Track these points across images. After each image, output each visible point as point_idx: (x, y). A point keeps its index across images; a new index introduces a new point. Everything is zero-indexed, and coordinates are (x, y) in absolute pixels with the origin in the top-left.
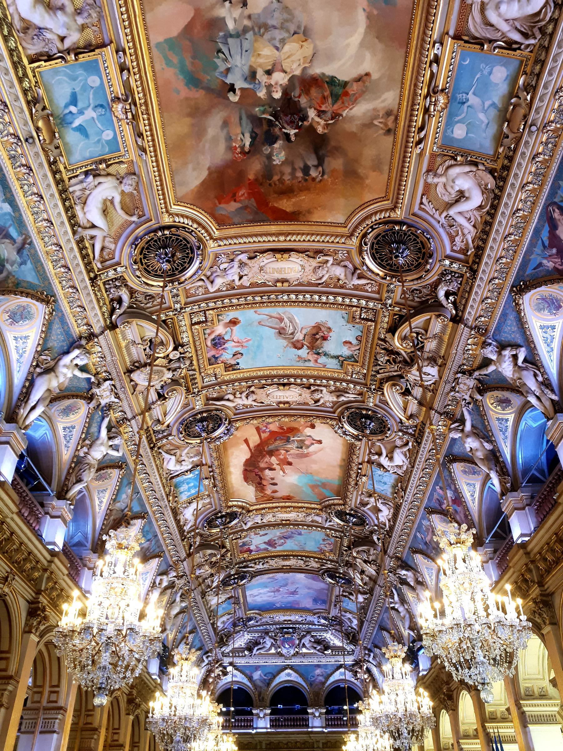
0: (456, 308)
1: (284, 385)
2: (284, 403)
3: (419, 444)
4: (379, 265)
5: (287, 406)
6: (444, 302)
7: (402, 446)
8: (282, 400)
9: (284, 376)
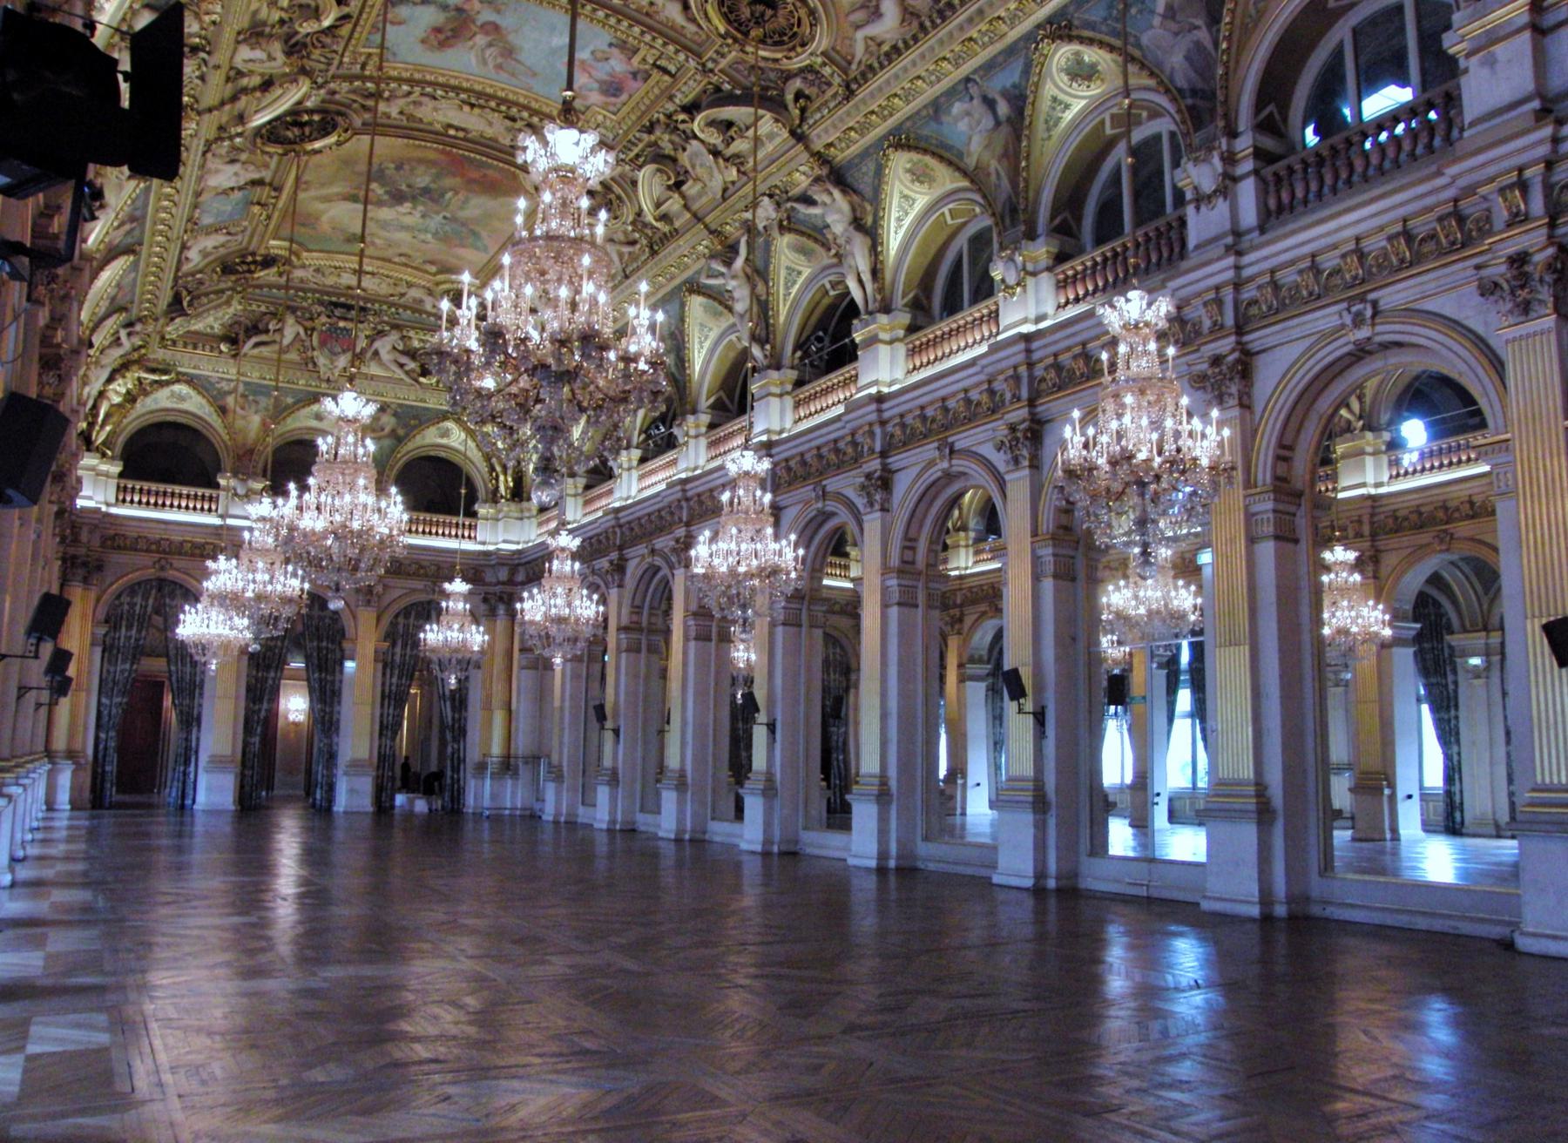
0: (803, 119)
1: (472, 106)
2: (457, 129)
3: (654, 253)
4: (725, 16)
5: (461, 134)
6: (791, 105)
7: (621, 243)
8: (456, 123)
9: (480, 95)
